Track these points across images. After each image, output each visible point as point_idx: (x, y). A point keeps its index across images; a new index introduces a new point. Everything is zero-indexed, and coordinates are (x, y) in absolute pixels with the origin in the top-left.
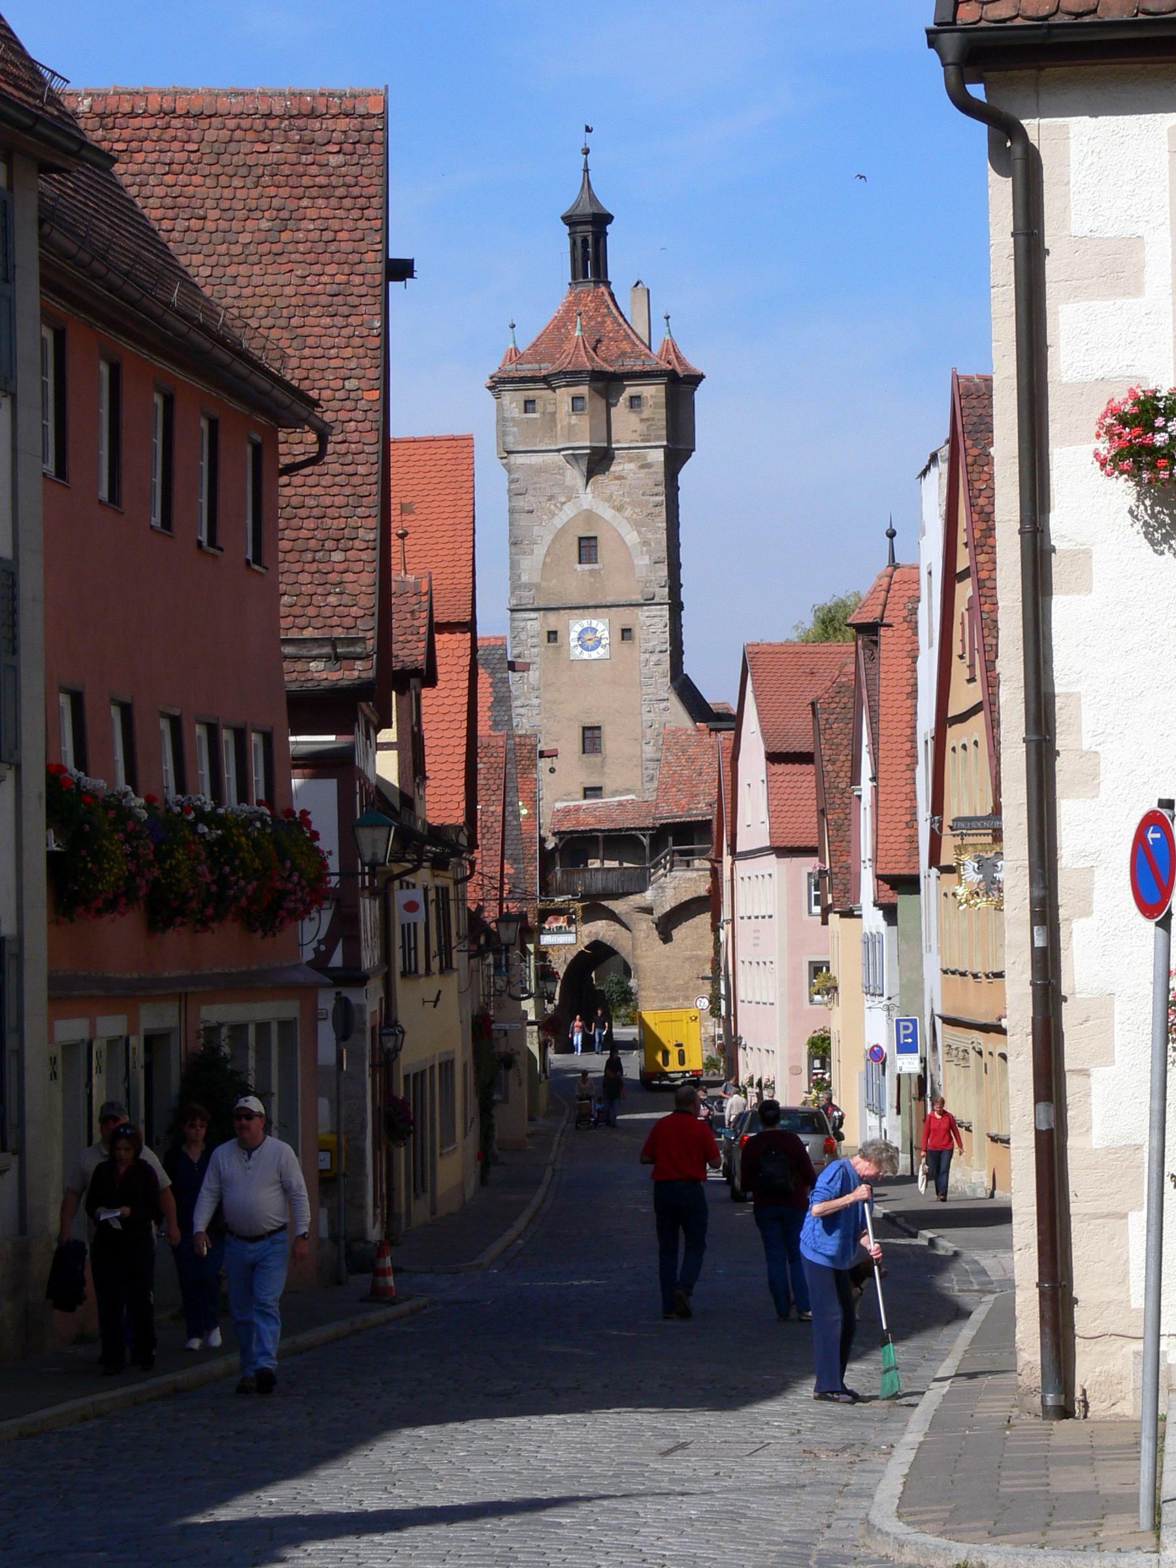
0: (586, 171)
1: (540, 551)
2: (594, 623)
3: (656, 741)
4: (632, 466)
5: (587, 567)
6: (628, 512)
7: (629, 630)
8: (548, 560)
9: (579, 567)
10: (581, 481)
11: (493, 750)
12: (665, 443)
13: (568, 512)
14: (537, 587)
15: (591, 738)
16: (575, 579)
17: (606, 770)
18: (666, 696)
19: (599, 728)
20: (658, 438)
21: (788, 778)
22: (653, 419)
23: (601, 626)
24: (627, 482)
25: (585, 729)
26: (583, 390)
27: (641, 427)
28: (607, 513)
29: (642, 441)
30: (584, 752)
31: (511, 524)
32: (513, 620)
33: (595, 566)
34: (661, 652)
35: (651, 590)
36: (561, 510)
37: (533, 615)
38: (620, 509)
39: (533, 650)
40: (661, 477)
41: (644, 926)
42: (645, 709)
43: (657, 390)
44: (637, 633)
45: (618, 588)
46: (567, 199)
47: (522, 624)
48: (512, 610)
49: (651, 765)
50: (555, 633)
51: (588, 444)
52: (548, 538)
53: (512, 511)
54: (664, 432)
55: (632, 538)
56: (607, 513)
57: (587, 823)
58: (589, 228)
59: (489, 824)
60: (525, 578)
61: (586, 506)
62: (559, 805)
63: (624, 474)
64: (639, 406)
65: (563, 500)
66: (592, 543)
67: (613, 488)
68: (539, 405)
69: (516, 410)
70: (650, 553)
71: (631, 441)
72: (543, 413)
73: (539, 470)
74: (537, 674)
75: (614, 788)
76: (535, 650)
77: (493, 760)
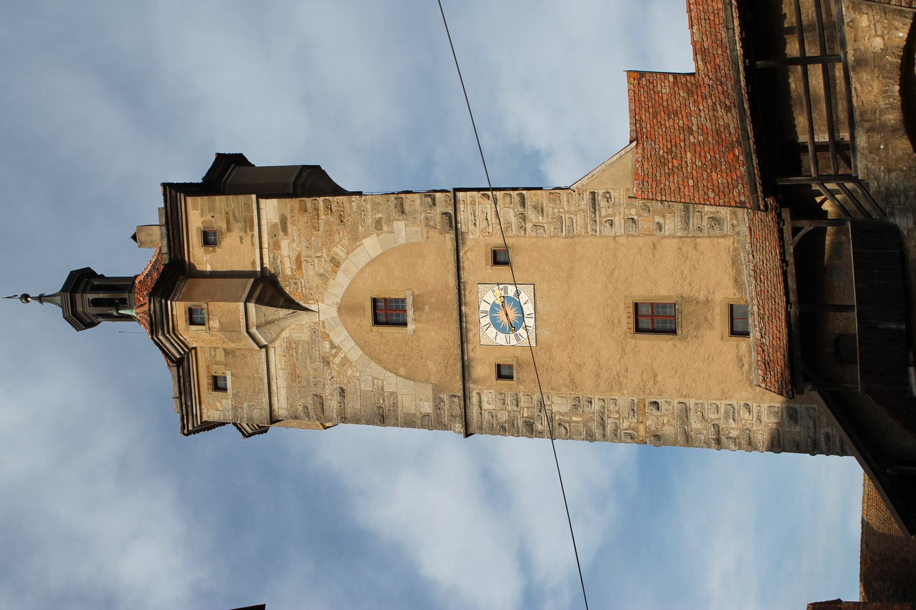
0: (41, 298)
1: (392, 383)
2: (485, 307)
3: (657, 212)
4: (284, 244)
5: (410, 314)
6: (339, 251)
7: (495, 253)
8: (402, 371)
9: (411, 326)
10: (303, 318)
12: (254, 197)
13: (340, 336)
14: (437, 389)
15: (655, 320)
16: (427, 333)
17: (702, 298)
18: (587, 196)
19: (636, 305)
22: (227, 213)
23: (489, 296)
24: (304, 253)
25: (638, 330)
26: (178, 309)
27: (236, 234)
28: (341, 282)
29: (252, 229)
30: (673, 332)
31: (357, 421)
32: (481, 430)
33: (409, 302)
34: (523, 204)
35: (438, 218)
36: (338, 348)
37: (475, 399)
38: (336, 263)
39: (522, 404)
40: (295, 203)
42: (607, 231)
43: (195, 208)
45: (434, 272)
47: (486, 415)
48: (467, 434)
49: (694, 221)
50: (499, 367)
51: (242, 304)
52: (377, 370)
53: (344, 420)
54: (242, 198)
55: (371, 246)
56: (341, 282)
58: (78, 297)
60: (427, 408)
61: (334, 312)
63: (294, 256)
64: (215, 233)
65: (327, 345)
66: (381, 305)
67: (311, 272)
68: (219, 371)
69: (224, 402)
70: (390, 222)
71: (253, 244)
72: (226, 365)
73: (294, 376)
74: (556, 399)
75: (731, 284)
76: (523, 398)
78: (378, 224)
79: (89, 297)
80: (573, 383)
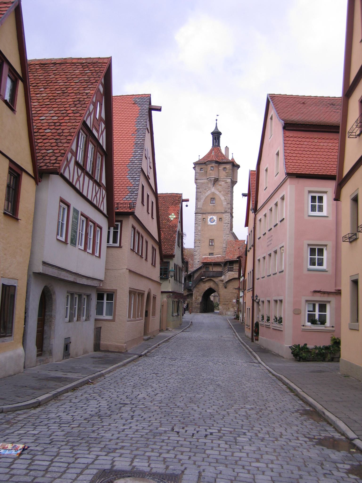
0: (216, 124)
1: (202, 201)
4: (223, 183)
6: (222, 193)
9: (211, 204)
13: (209, 192)
14: (201, 208)
20: (229, 177)
21: (295, 139)
23: (215, 218)
27: (226, 174)
28: (217, 193)
38: (220, 192)
41: (221, 285)
44: (223, 219)
46: (213, 129)
52: (204, 198)
53: (196, 192)
55: (223, 198)
56: (217, 193)
57: (209, 261)
60: (198, 207)
62: (203, 257)
70: (226, 201)
73: (203, 183)
78: (226, 199)
79: (216, 135)
80: (202, 230)
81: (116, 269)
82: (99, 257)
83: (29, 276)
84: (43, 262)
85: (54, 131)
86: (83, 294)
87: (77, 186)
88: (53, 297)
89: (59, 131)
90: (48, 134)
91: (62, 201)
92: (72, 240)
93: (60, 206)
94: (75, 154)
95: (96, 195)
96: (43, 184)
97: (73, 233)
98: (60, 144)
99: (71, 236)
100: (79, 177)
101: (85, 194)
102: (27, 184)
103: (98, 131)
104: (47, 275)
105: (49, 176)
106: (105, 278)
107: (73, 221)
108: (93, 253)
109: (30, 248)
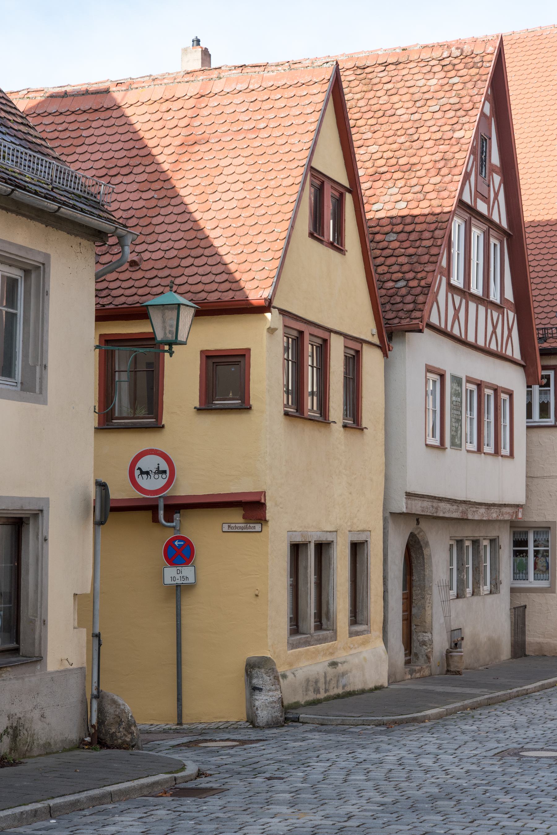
11: (477, 59)
59: (449, 155)
77: (474, 71)
81: (549, 477)
82: (512, 455)
83: (385, 520)
84: (406, 493)
85: (403, 236)
86: (481, 538)
87: (456, 332)
88: (425, 552)
89: (413, 237)
90: (392, 245)
91: (429, 369)
92: (453, 438)
93: (427, 380)
94: (448, 273)
95: (494, 332)
96: (396, 348)
97: (454, 424)
98: (419, 268)
99: (451, 430)
100: (457, 311)
101: (471, 339)
102: (372, 360)
103: (486, 200)
104: (414, 514)
105: (404, 336)
106: (527, 497)
107: (452, 402)
108: (497, 452)
109: (384, 472)
